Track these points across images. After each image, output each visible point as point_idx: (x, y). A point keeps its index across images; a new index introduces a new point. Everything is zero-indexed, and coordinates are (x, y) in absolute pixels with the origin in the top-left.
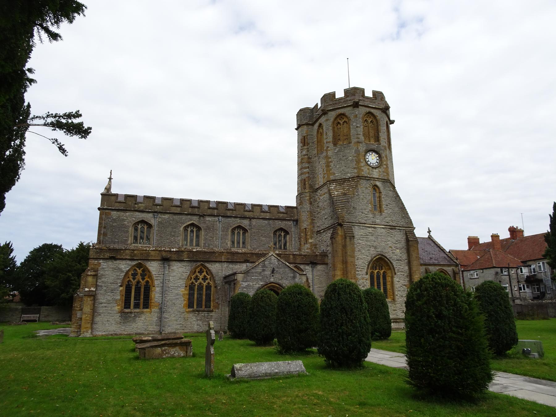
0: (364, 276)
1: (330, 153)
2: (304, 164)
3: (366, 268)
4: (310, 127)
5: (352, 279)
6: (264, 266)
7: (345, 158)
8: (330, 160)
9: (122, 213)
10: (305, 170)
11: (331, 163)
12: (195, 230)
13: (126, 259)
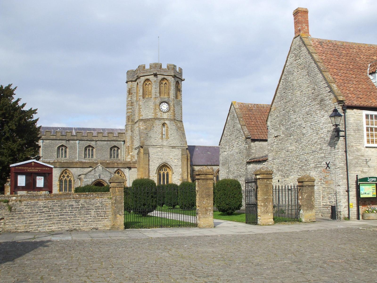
1: (141, 103)
6: (95, 171)
8: (140, 107)
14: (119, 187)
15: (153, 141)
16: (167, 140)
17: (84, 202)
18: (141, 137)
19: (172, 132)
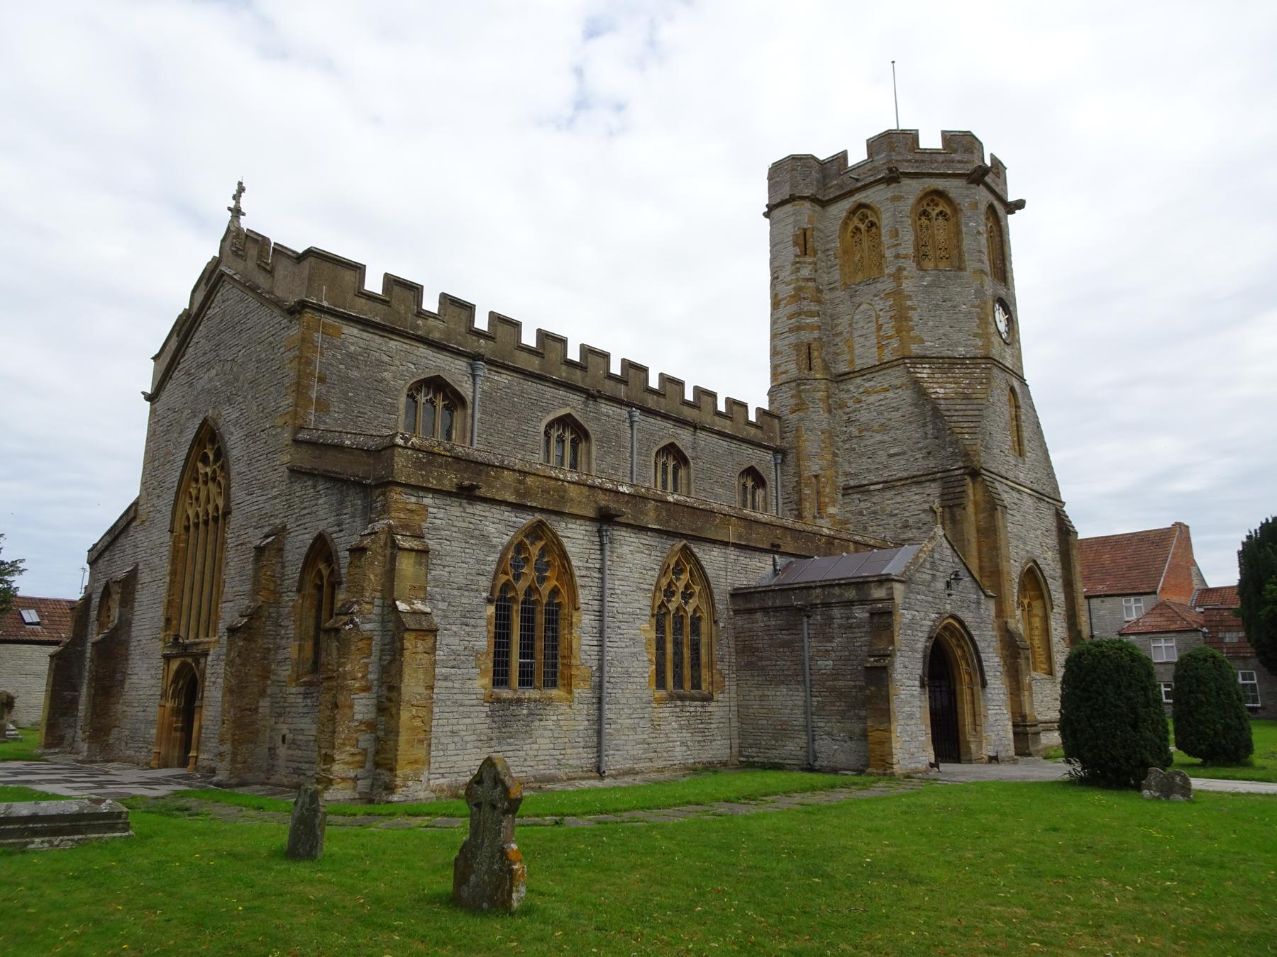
2: (805, 302)
7: (949, 304)
8: (909, 303)
11: (911, 313)
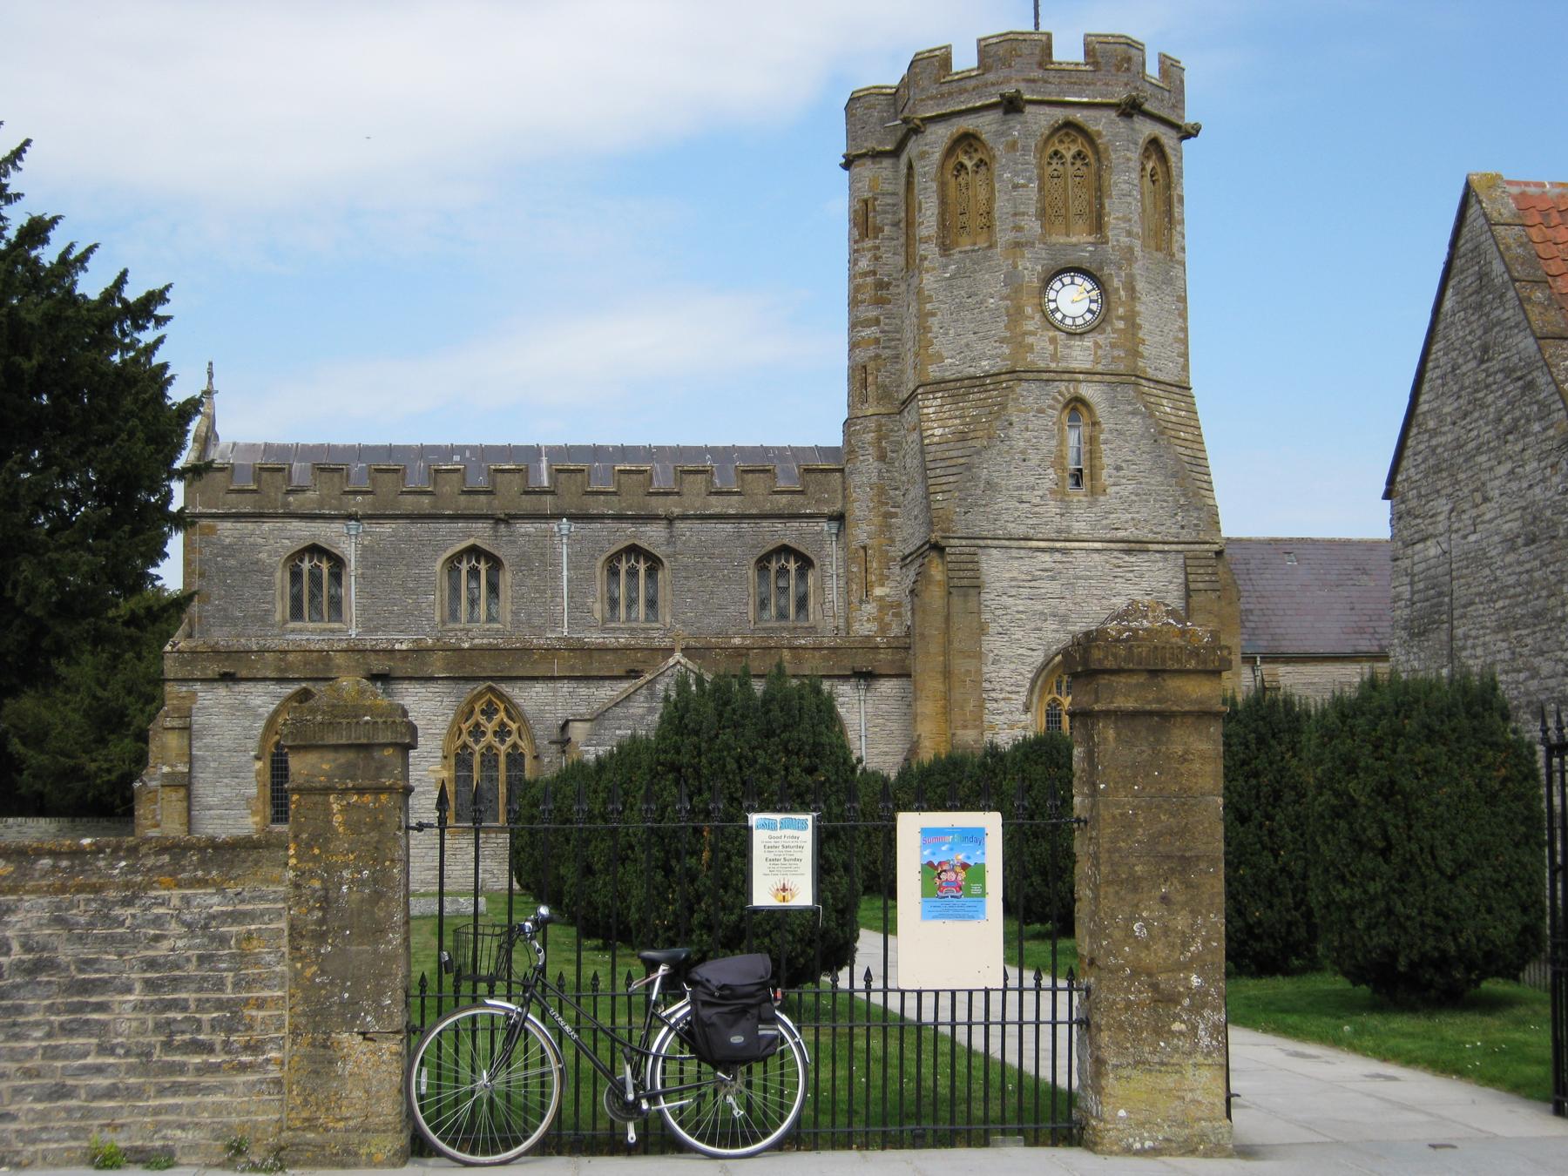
0: (1017, 716)
3: (1024, 691)
4: (887, 163)
5: (965, 727)
8: (929, 306)
9: (250, 526)
10: (866, 332)
11: (931, 320)
12: (483, 567)
13: (265, 679)
14: (361, 791)
15: (1009, 514)
16: (1091, 505)
17: (48, 926)
18: (932, 489)
19: (1125, 453)
